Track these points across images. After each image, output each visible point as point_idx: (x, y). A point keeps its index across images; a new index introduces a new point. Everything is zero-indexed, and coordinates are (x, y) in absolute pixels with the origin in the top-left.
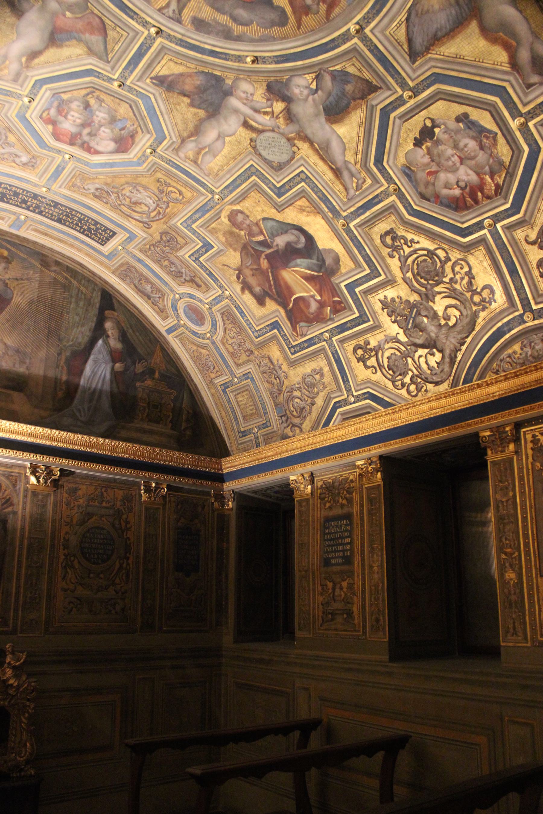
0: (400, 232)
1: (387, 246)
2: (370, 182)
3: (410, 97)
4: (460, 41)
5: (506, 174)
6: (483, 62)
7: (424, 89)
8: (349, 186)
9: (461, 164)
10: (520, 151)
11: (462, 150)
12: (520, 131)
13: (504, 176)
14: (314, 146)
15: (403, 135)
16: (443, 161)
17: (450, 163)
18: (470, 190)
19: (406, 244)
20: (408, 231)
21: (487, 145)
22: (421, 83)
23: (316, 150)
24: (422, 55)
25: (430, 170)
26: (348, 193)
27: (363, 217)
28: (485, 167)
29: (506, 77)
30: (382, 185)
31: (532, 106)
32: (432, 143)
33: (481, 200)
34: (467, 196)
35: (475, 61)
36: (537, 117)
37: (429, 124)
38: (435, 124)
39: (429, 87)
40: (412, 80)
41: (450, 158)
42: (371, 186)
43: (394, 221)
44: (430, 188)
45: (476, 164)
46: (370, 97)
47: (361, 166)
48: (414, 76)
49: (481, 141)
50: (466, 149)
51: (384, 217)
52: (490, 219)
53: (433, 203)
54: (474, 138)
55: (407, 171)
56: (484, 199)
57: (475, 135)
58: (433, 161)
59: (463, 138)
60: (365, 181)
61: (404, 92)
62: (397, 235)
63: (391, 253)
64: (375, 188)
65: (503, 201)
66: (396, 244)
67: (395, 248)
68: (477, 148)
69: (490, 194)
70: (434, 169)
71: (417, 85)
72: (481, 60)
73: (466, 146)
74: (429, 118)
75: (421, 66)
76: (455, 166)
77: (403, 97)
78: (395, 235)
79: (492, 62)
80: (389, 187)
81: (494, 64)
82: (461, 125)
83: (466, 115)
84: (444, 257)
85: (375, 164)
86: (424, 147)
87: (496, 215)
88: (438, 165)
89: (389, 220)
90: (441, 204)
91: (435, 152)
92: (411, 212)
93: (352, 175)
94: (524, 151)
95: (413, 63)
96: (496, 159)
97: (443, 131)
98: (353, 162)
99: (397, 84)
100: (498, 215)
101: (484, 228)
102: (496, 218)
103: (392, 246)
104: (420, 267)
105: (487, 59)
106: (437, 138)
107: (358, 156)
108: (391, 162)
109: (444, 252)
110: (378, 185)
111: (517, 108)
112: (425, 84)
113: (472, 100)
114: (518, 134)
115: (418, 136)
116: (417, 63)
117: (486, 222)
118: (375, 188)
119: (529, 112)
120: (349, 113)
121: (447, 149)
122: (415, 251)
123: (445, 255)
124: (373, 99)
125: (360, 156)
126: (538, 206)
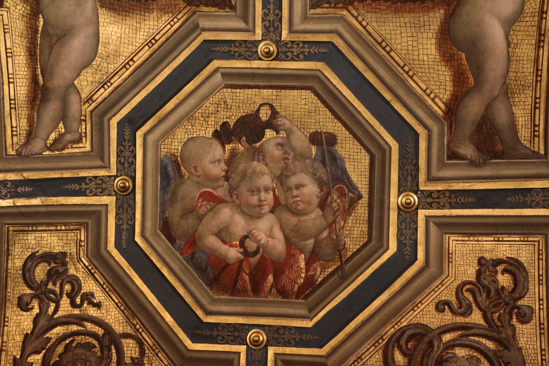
0: (76, 269)
1: (29, 282)
2: (88, 148)
3: (268, 54)
4: (403, 25)
5: (336, 270)
6: (411, 77)
7: (298, 56)
8: (42, 134)
9: (272, 211)
10: (383, 246)
11: (290, 189)
12: (399, 214)
13: (330, 270)
14: (37, 20)
15: (209, 106)
16: (243, 189)
17: (254, 200)
18: (258, 263)
19: (71, 297)
20: (93, 275)
21: (334, 204)
22: (301, 45)
23: (32, 30)
24: (335, 4)
25: (211, 191)
26: (27, 143)
27: (20, 202)
28: (307, 239)
29: (429, 122)
30: (107, 167)
31: (440, 187)
32: (247, 150)
33: (266, 289)
34: (247, 271)
35: (402, 68)
36: (439, 208)
37: (265, 115)
38: (275, 121)
39: (307, 58)
40: (291, 31)
41: (259, 191)
42: (85, 155)
43: (78, 244)
44: (191, 221)
45: (296, 226)
46: (204, 9)
47: (92, 112)
48: (298, 25)
49: (329, 194)
50: (295, 193)
51: (65, 224)
52: (264, 330)
53: (178, 249)
54: (320, 183)
55: (170, 168)
56: (274, 290)
57: (325, 178)
58: (227, 178)
59: (302, 171)
60: (80, 141)
61: (263, 40)
62: (66, 270)
63: (26, 299)
64: (87, 164)
65: (304, 312)
66: (50, 286)
67: (44, 293)
68: (316, 201)
69: (288, 287)
70: (220, 193)
71: (292, 42)
72: (411, 73)
73: (298, 187)
74: (272, 107)
75: (321, 19)
76: (258, 209)
77: (257, 47)
78: (61, 269)
79: (424, 87)
80: (116, 177)
81: (425, 91)
82: (314, 149)
83: (332, 139)
84: (132, 358)
85: (120, 124)
86: (228, 147)
87: (278, 329)
88: (232, 190)
89: (71, 235)
90: (192, 259)
91: (241, 167)
92: (124, 244)
93: (63, 117)
94: (388, 249)
95: (313, 7)
96: (335, 237)
97: (279, 141)
98: (84, 96)
99: (263, 20)
100: (281, 332)
101: (243, 342)
102: (276, 336)
103: (40, 286)
104: (70, 354)
105: (420, 78)
106: (261, 146)
107: (102, 90)
108: (151, 138)
109: (137, 350)
110: (99, 163)
111: (416, 177)
112: (307, 50)
113: (358, 122)
114: (393, 216)
115: (232, 124)
116: (319, 11)
117: (251, 335)
118: (87, 164)
119: (431, 193)
120: (149, 10)
121: (263, 174)
122: (80, 320)
123: (137, 355)
124: (207, 16)
125: (106, 94)
126: (360, 352)
